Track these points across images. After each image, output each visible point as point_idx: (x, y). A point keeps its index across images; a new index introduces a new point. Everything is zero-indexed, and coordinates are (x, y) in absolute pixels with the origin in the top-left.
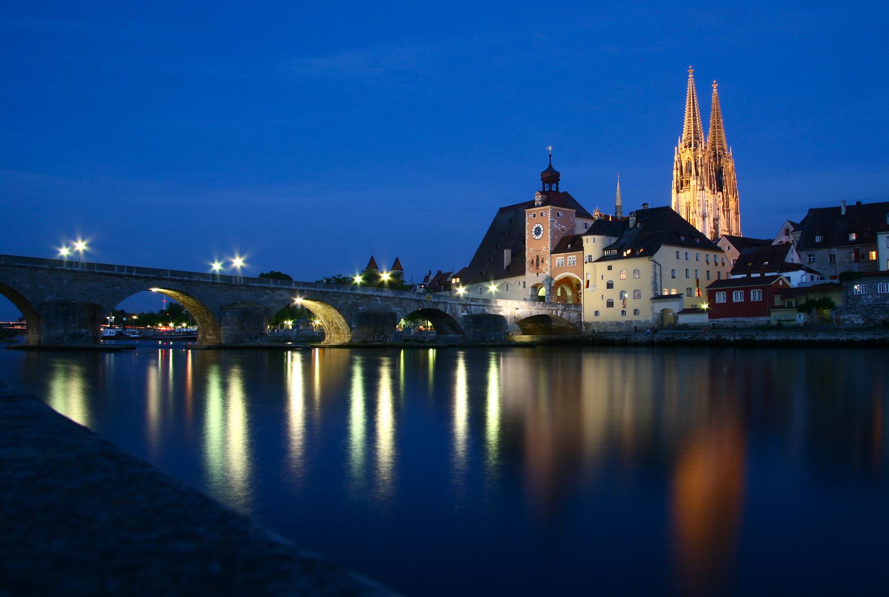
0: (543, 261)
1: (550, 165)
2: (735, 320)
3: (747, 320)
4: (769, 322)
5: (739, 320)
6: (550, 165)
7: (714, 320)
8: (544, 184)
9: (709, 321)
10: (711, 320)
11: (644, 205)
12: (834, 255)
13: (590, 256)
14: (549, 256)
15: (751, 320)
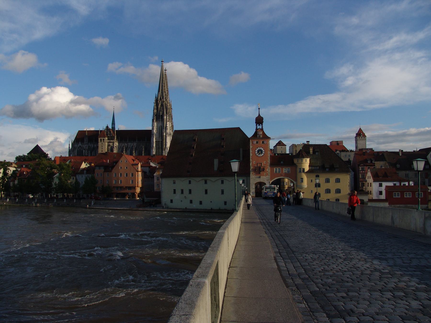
0: (263, 170)
1: (259, 114)
2: (406, 206)
3: (414, 206)
4: (428, 207)
5: (409, 206)
6: (259, 114)
7: (392, 205)
8: (256, 125)
9: (389, 206)
10: (390, 205)
11: (307, 142)
12: (408, 174)
13: (304, 169)
14: (269, 168)
15: (416, 206)
